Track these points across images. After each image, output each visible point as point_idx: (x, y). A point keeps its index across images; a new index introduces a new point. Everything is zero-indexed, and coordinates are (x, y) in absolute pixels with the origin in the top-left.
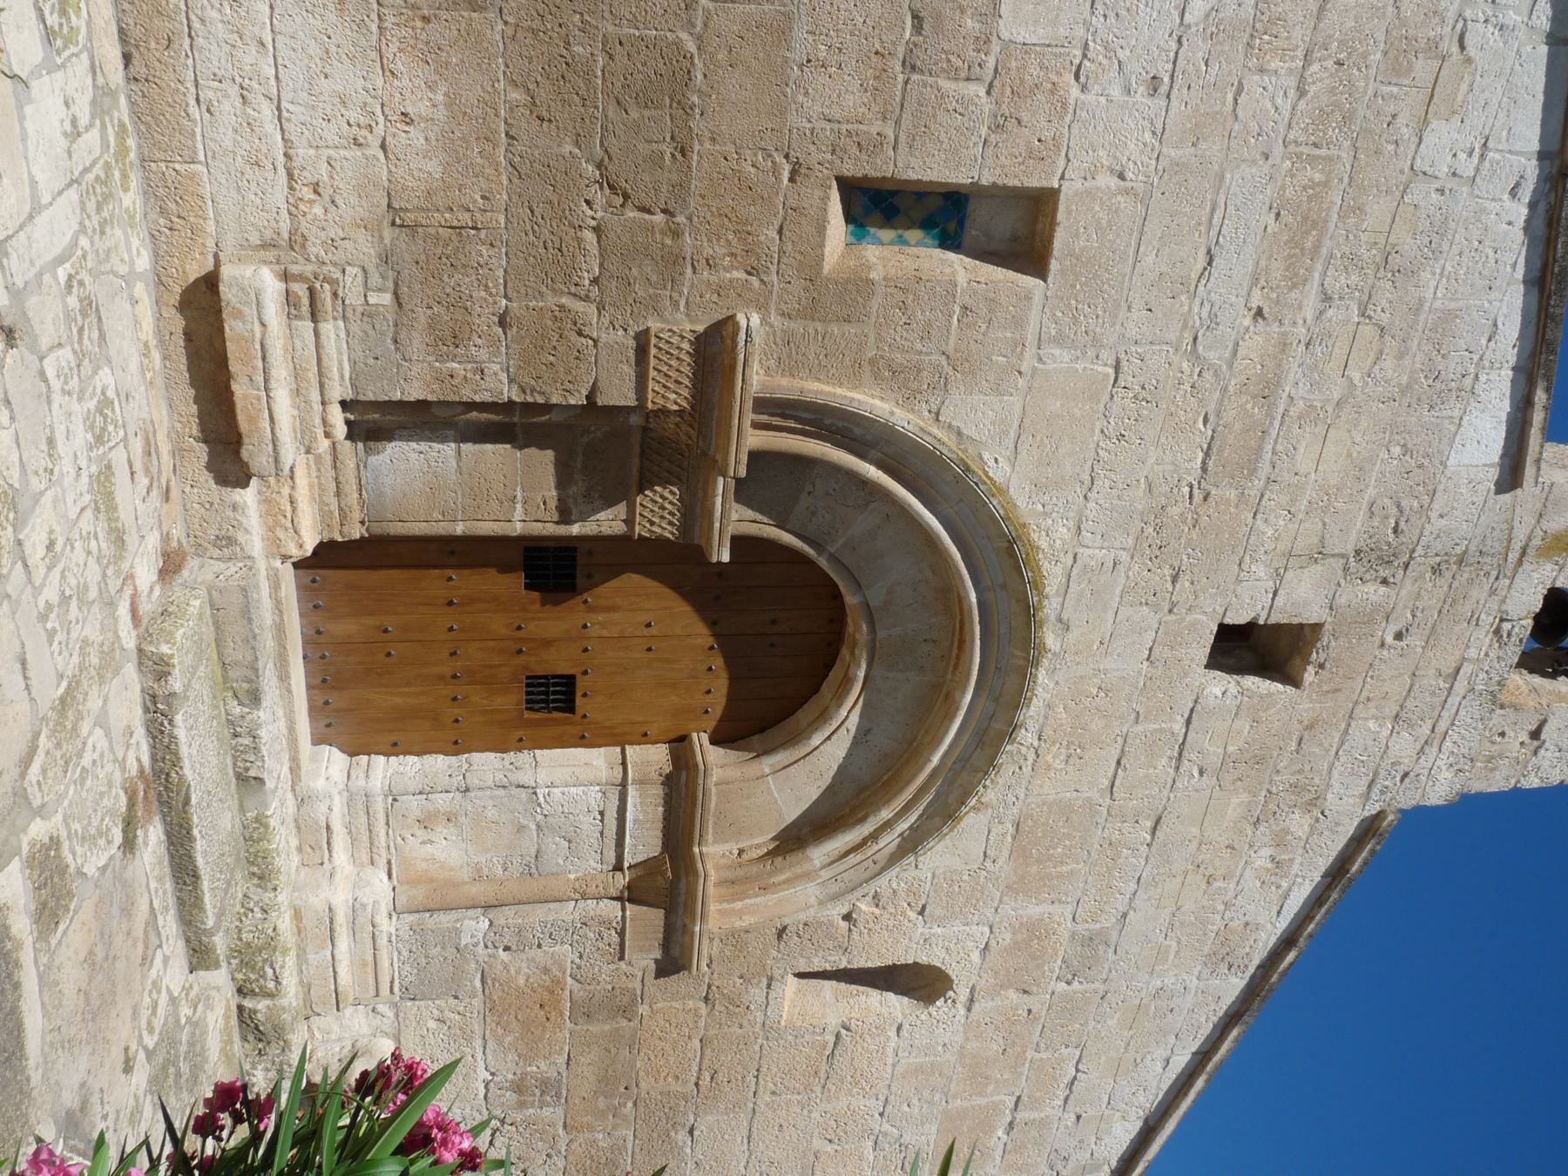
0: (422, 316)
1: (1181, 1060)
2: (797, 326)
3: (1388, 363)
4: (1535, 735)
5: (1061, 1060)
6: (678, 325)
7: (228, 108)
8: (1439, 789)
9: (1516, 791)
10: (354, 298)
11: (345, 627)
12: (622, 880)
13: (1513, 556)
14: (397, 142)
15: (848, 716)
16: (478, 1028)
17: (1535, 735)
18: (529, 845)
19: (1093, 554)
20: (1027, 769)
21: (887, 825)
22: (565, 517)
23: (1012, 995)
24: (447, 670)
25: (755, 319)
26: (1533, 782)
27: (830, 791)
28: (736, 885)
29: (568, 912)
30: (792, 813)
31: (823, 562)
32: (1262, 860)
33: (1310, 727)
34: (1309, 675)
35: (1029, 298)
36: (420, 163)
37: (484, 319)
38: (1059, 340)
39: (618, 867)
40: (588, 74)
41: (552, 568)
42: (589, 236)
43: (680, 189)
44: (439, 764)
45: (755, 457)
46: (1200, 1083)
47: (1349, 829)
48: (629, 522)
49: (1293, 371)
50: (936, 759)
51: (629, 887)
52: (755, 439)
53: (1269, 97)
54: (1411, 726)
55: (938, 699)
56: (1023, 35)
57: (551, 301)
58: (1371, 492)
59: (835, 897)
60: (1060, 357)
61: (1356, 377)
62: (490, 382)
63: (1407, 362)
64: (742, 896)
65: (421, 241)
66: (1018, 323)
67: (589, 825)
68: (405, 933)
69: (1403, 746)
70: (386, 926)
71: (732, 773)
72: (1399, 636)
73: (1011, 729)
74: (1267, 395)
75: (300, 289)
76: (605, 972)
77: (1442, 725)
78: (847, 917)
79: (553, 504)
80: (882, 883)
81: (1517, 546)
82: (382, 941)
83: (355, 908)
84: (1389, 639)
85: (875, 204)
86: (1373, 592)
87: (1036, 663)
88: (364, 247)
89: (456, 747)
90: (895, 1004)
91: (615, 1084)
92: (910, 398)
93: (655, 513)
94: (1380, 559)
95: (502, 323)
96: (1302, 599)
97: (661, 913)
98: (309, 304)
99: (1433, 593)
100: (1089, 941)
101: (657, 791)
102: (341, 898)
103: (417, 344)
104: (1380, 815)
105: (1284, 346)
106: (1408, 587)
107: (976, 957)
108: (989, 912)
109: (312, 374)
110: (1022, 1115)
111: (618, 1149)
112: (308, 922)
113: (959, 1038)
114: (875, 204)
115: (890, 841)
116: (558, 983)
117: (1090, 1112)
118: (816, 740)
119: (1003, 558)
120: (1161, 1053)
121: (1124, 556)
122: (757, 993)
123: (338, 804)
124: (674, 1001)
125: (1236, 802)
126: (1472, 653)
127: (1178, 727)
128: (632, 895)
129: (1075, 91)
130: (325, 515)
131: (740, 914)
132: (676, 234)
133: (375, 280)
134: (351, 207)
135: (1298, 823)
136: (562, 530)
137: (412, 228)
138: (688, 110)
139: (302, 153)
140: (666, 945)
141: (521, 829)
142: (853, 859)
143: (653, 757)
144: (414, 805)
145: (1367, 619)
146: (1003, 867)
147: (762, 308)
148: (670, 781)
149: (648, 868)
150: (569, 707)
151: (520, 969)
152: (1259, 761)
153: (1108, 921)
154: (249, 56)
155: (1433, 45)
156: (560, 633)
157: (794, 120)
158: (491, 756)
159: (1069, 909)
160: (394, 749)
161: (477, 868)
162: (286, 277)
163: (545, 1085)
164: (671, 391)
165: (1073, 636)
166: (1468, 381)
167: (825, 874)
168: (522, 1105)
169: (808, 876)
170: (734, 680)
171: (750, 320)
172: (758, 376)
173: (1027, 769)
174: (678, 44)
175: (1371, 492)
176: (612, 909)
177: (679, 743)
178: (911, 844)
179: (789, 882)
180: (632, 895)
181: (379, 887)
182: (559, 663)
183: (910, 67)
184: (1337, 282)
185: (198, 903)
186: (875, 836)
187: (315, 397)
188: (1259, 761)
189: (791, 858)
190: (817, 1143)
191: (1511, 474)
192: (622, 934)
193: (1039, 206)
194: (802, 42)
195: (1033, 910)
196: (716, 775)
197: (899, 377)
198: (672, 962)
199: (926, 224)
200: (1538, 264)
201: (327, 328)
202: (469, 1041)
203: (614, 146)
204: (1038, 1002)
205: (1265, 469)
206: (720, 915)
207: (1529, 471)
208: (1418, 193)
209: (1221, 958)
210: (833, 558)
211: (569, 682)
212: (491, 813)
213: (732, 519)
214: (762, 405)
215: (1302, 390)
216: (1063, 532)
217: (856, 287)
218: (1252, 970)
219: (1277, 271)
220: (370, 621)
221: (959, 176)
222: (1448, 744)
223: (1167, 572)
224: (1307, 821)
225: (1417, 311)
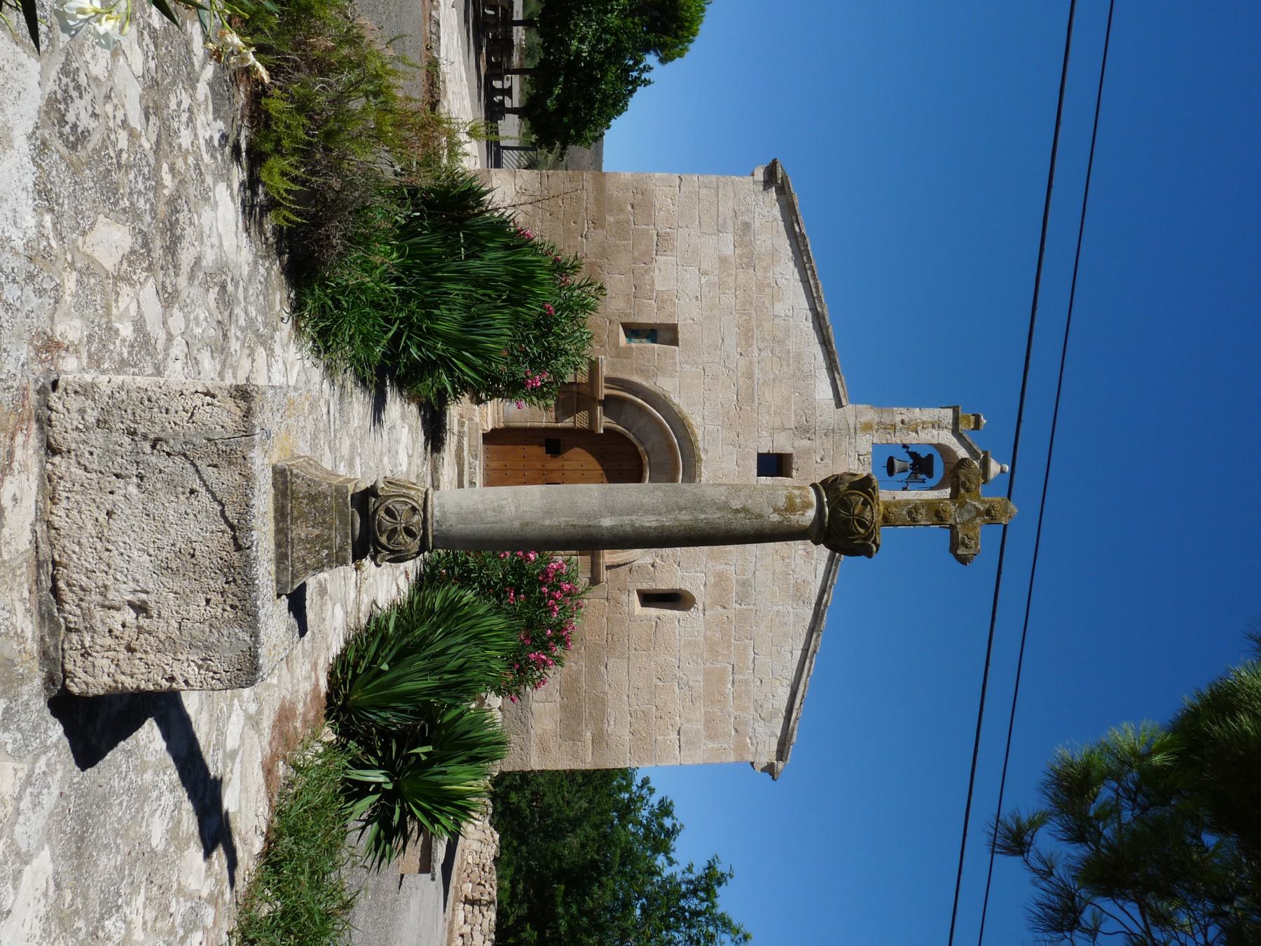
1: (798, 654)
11: (494, 465)
13: (852, 431)
19: (710, 427)
23: (721, 610)
31: (631, 436)
34: (794, 473)
38: (686, 362)
49: (756, 371)
52: (606, 391)
53: (729, 299)
66: (673, 358)
81: (852, 427)
85: (633, 331)
86: (806, 443)
92: (647, 378)
93: (580, 420)
94: (805, 430)
96: (782, 444)
99: (828, 444)
107: (702, 587)
110: (738, 677)
111: (579, 672)
114: (633, 331)
119: (681, 425)
120: (788, 648)
145: (808, 452)
153: (749, 575)
155: (769, 285)
165: (710, 454)
172: (605, 371)
184: (762, 345)
190: (655, 680)
193: (673, 329)
195: (720, 567)
197: (642, 372)
199: (647, 337)
204: (730, 613)
214: (608, 380)
215: (761, 376)
217: (627, 352)
220: (502, 463)
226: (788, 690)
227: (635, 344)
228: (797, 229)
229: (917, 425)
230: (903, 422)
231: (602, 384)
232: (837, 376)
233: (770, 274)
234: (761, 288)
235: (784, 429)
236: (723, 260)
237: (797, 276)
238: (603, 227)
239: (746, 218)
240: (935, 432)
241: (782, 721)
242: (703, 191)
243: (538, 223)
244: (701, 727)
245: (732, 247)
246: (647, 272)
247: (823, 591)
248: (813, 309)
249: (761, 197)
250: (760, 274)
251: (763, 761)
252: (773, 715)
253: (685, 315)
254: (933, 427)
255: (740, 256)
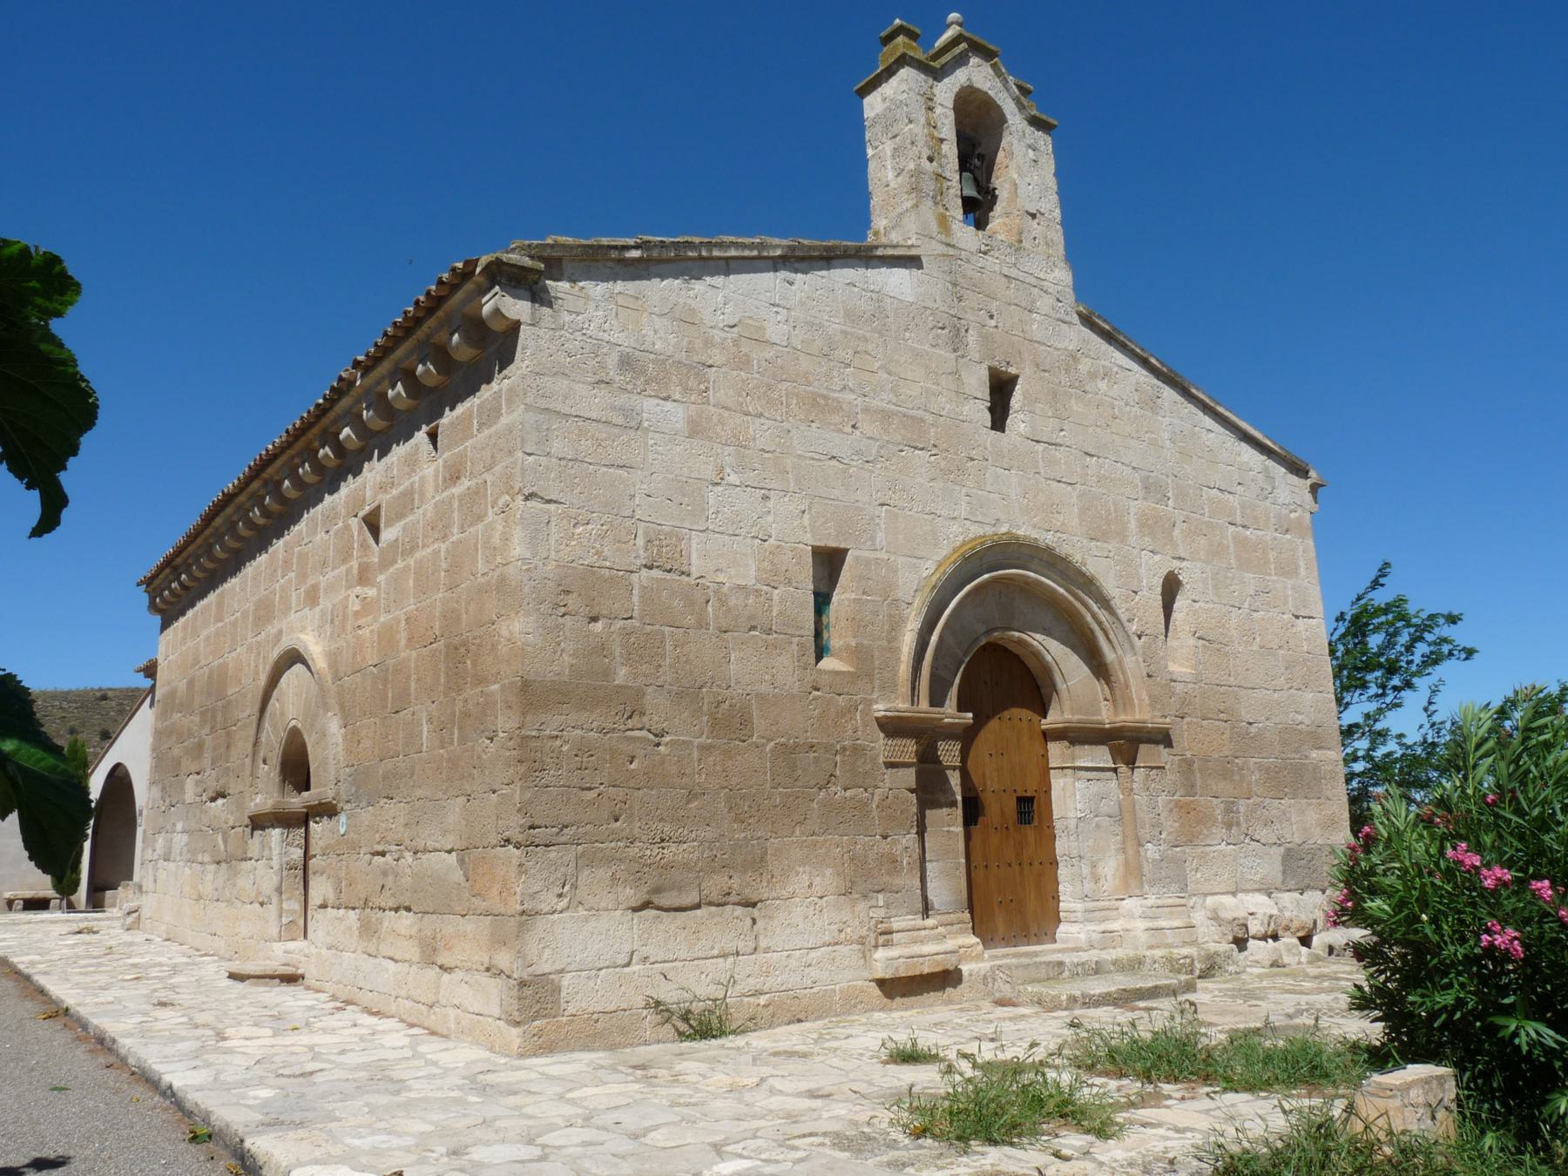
0: (886, 878)
1: (1208, 422)
2: (877, 683)
3: (870, 347)
4: (1033, 216)
5: (1209, 499)
6: (881, 746)
7: (814, 973)
8: (1062, 276)
9: (1062, 224)
10: (881, 913)
12: (1123, 768)
13: (951, 251)
14: (818, 889)
15: (1038, 640)
16: (1200, 850)
17: (1033, 216)
18: (1105, 821)
20: (1064, 536)
21: (1094, 616)
22: (953, 804)
23: (1176, 533)
24: (1016, 868)
25: (880, 707)
26: (1057, 212)
27: (1074, 649)
28: (1128, 704)
29: (1141, 798)
30: (1084, 670)
32: (1102, 385)
33: (1037, 365)
34: (1013, 370)
35: (857, 558)
36: (826, 880)
37: (885, 846)
38: (873, 539)
39: (1115, 770)
40: (788, 795)
41: (973, 811)
42: (849, 793)
43: (828, 748)
44: (1063, 872)
45: (932, 705)
46: (1220, 409)
47: (1086, 332)
48: (954, 768)
49: (876, 403)
50: (1061, 590)
51: (1127, 764)
52: (924, 704)
53: (761, 433)
54: (1034, 301)
55: (1025, 587)
56: (753, 573)
57: (875, 813)
58: (927, 347)
59: (1132, 646)
60: (880, 536)
61: (877, 365)
62: (910, 844)
63: (868, 335)
64: (1131, 699)
65: (860, 881)
66: (868, 562)
67: (1095, 787)
68: (1155, 890)
69: (1045, 304)
70: (1152, 901)
71: (1067, 705)
72: (991, 317)
73: (1049, 551)
74: (886, 416)
75: (881, 939)
76: (1171, 777)
77: (1034, 282)
78: (1139, 637)
79: (949, 810)
80: (1124, 618)
82: (1160, 902)
83: (1145, 917)
84: (993, 323)
86: (972, 338)
87: (1017, 538)
88: (862, 906)
89: (1054, 863)
90: (1180, 603)
91: (1226, 770)
94: (956, 336)
95: (885, 838)
97: (1142, 746)
98: (886, 935)
99: (972, 299)
100: (1147, 488)
101: (1078, 749)
102: (1141, 925)
103: (898, 881)
104: (1080, 314)
105: (866, 410)
106: (968, 316)
107: (1157, 558)
108: (1135, 552)
109: (915, 934)
110: (1239, 520)
111: (1260, 767)
112: (1154, 942)
113: (1199, 564)
115: (1103, 615)
116: (1178, 805)
117: (1236, 477)
118: (1049, 658)
121: (964, 491)
122: (1179, 688)
123: (1091, 927)
124: (1183, 735)
125: (1076, 407)
126: (997, 268)
127: (1040, 447)
128: (1131, 762)
129: (771, 541)
130: (962, 932)
131: (1141, 700)
132: (844, 749)
133: (873, 902)
134: (846, 915)
135: (1085, 366)
136: (960, 805)
137: (853, 883)
138: (796, 745)
139: (827, 938)
140: (1157, 742)
141: (1098, 826)
142: (1112, 636)
143: (1056, 750)
144: (1089, 886)
145: (986, 339)
146: (1112, 545)
147: (872, 702)
148: (1073, 742)
149: (1116, 754)
150: (1031, 800)
151: (1170, 825)
152: (1055, 394)
153: (1137, 477)
154: (793, 963)
155: (736, 342)
156: (999, 807)
157: (795, 691)
158: (1058, 843)
159: (1133, 503)
160: (1056, 898)
161: (1118, 850)
162: (876, 947)
163: (1228, 811)
164: (908, 749)
165: (1002, 517)
166: (874, 296)
167: (1120, 652)
168: (1238, 824)
169: (1120, 662)
170: (1014, 705)
171: (880, 709)
173: (1064, 536)
174: (772, 751)
175: (927, 347)
176: (1139, 774)
177: (1048, 736)
178: (1105, 603)
179: (1124, 672)
180: (1131, 762)
181: (1129, 904)
182: (1011, 806)
183: (769, 631)
184: (837, 383)
185: (1167, 987)
186: (1100, 623)
187: (923, 933)
188: (1055, 394)
189: (1112, 671)
191: (913, 262)
192: (1152, 768)
194: (764, 688)
195: (1133, 525)
196: (1067, 716)
197: (896, 624)
198: (1163, 738)
200: (820, 263)
201: (895, 926)
202: (1207, 854)
203: (813, 782)
204: (1179, 516)
205: (920, 413)
206: (1140, 714)
207: (913, 252)
208: (797, 343)
209: (1152, 403)
210: (965, 655)
211: (1020, 800)
212: (1090, 843)
213: (950, 713)
215: (884, 396)
216: (955, 528)
217: (860, 655)
218: (1160, 383)
219: (836, 419)
221: (811, 598)
222: (1041, 275)
223: (970, 464)
224: (1084, 360)
225: (845, 333)
226: (1245, 447)
227: (836, 639)
228: (636, 254)
229: (933, 137)
230: (931, 159)
231: (936, 713)
232: (879, 252)
233: (718, 335)
234: (744, 363)
235: (956, 373)
236: (695, 429)
237: (718, 280)
238: (640, 694)
239: (612, 360)
240: (939, 110)
241: (1270, 463)
242: (557, 447)
243: (634, 851)
244: (1290, 583)
245: (669, 405)
246: (722, 601)
247: (1145, 363)
248: (776, 264)
249: (567, 318)
250: (717, 357)
251: (1309, 497)
252: (1270, 478)
253: (796, 530)
254: (930, 109)
255: (686, 390)
